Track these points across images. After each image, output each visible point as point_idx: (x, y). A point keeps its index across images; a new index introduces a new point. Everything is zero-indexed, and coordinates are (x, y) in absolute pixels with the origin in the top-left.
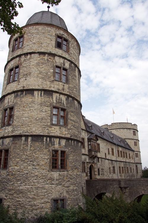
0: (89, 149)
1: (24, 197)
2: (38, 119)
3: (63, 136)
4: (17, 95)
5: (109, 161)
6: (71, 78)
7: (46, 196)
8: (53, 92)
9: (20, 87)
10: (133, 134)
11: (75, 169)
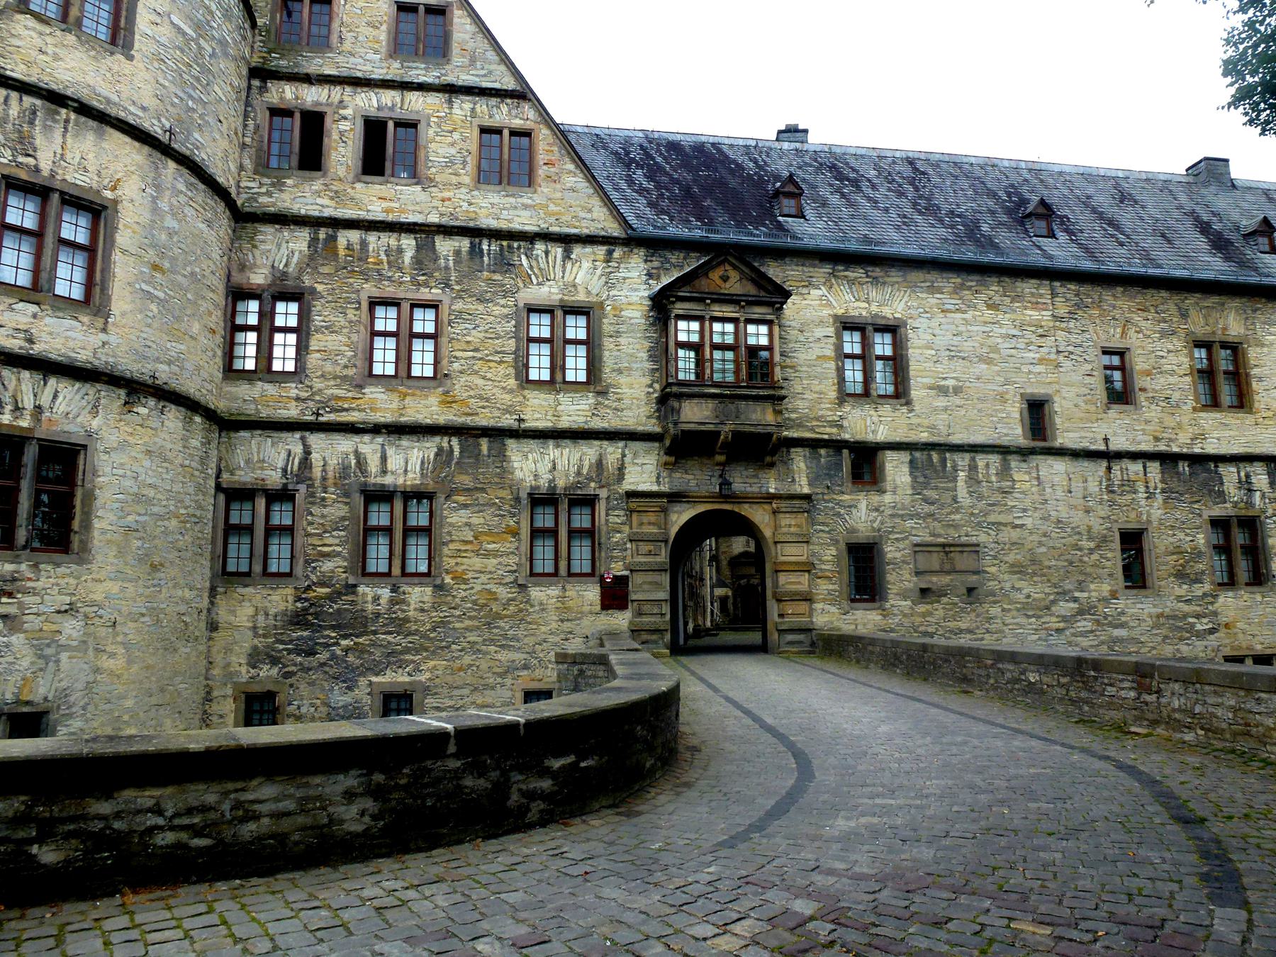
5: (1135, 467)
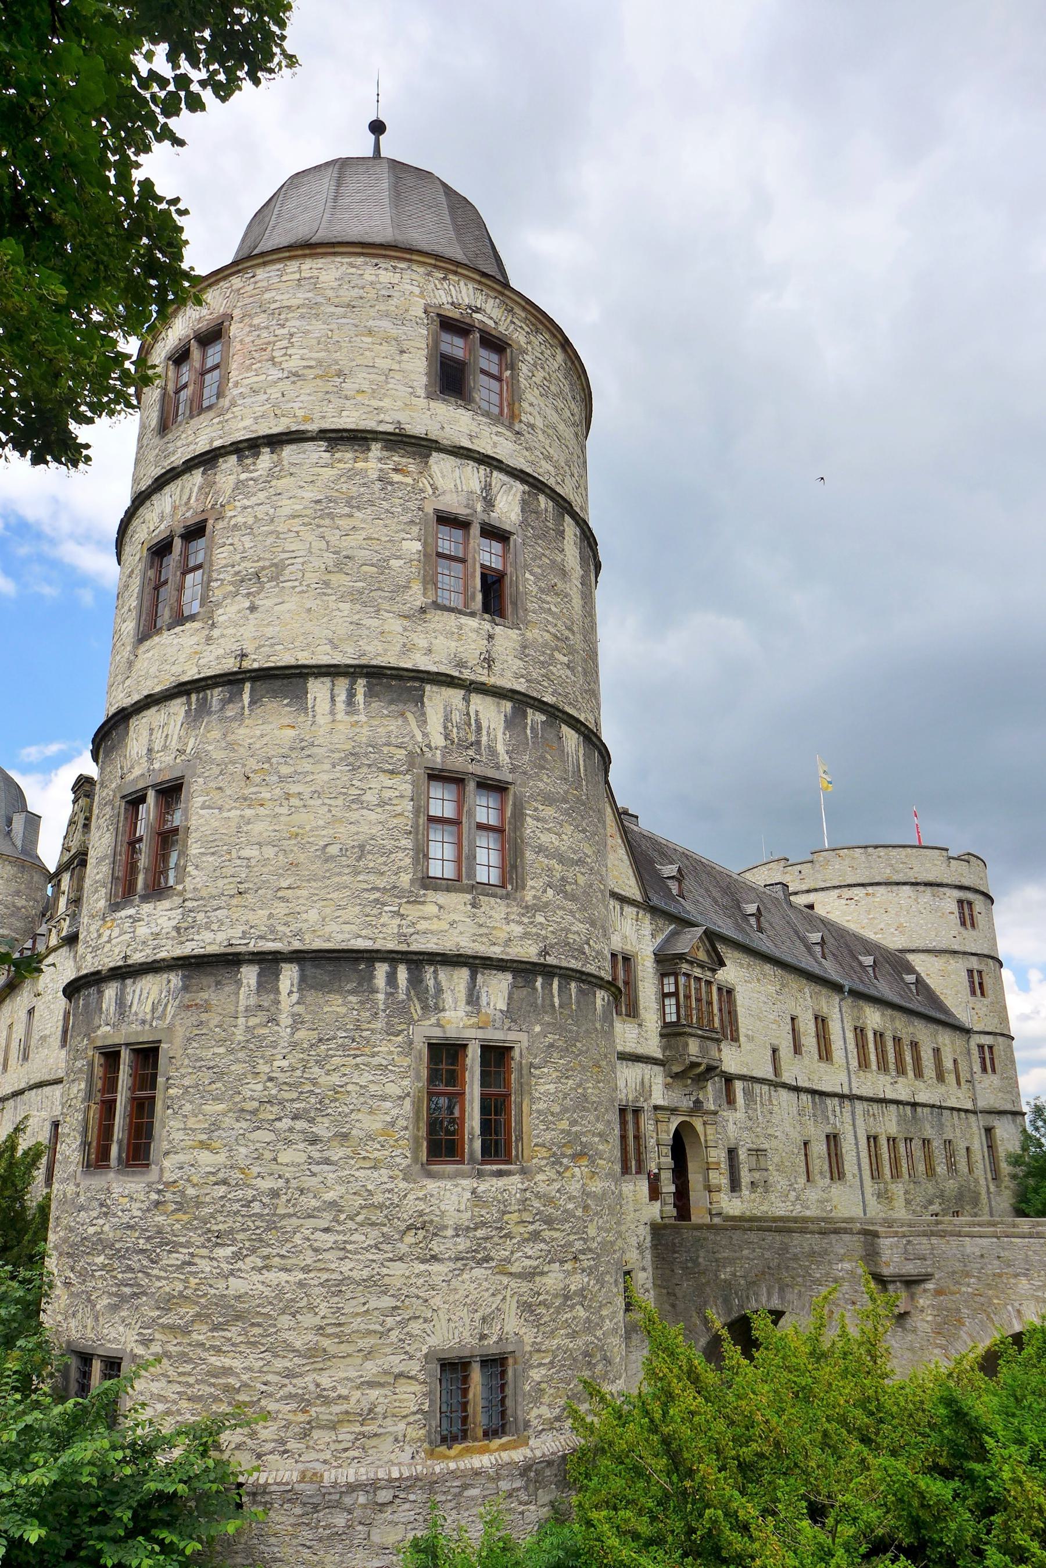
0: (666, 1025)
1: (254, 1344)
2: (334, 850)
3: (496, 952)
4: (203, 709)
5: (804, 1097)
6: (534, 589)
7: (394, 1334)
8: (422, 680)
9: (216, 660)
10: (955, 918)
11: (575, 1157)
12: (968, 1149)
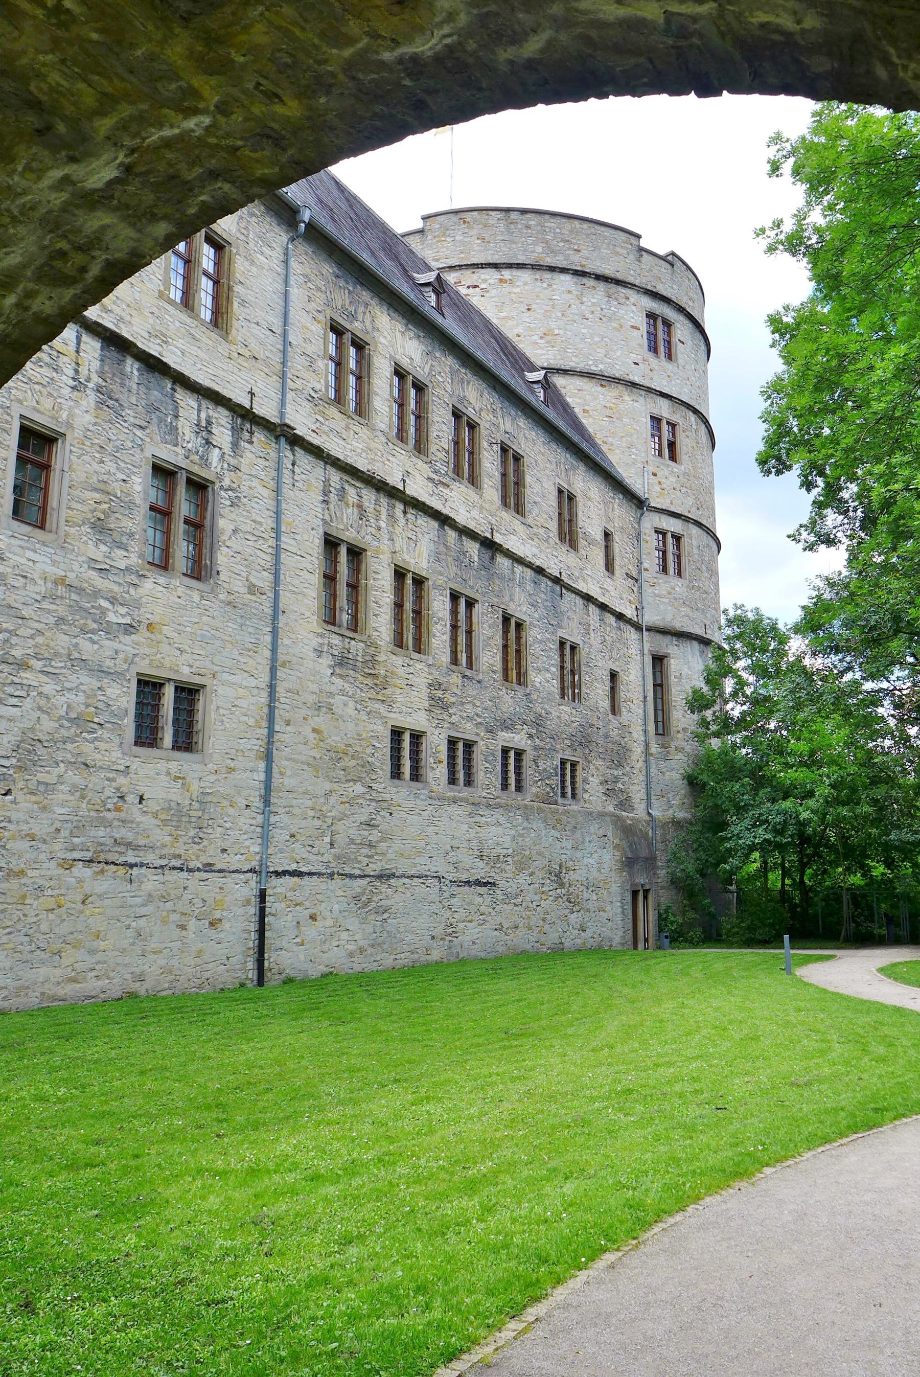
10: (640, 338)
12: (613, 676)
